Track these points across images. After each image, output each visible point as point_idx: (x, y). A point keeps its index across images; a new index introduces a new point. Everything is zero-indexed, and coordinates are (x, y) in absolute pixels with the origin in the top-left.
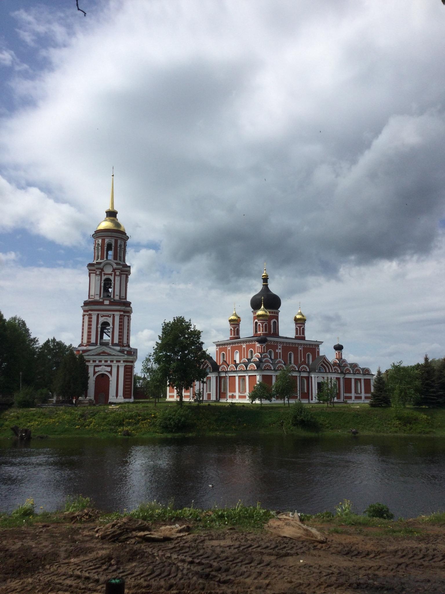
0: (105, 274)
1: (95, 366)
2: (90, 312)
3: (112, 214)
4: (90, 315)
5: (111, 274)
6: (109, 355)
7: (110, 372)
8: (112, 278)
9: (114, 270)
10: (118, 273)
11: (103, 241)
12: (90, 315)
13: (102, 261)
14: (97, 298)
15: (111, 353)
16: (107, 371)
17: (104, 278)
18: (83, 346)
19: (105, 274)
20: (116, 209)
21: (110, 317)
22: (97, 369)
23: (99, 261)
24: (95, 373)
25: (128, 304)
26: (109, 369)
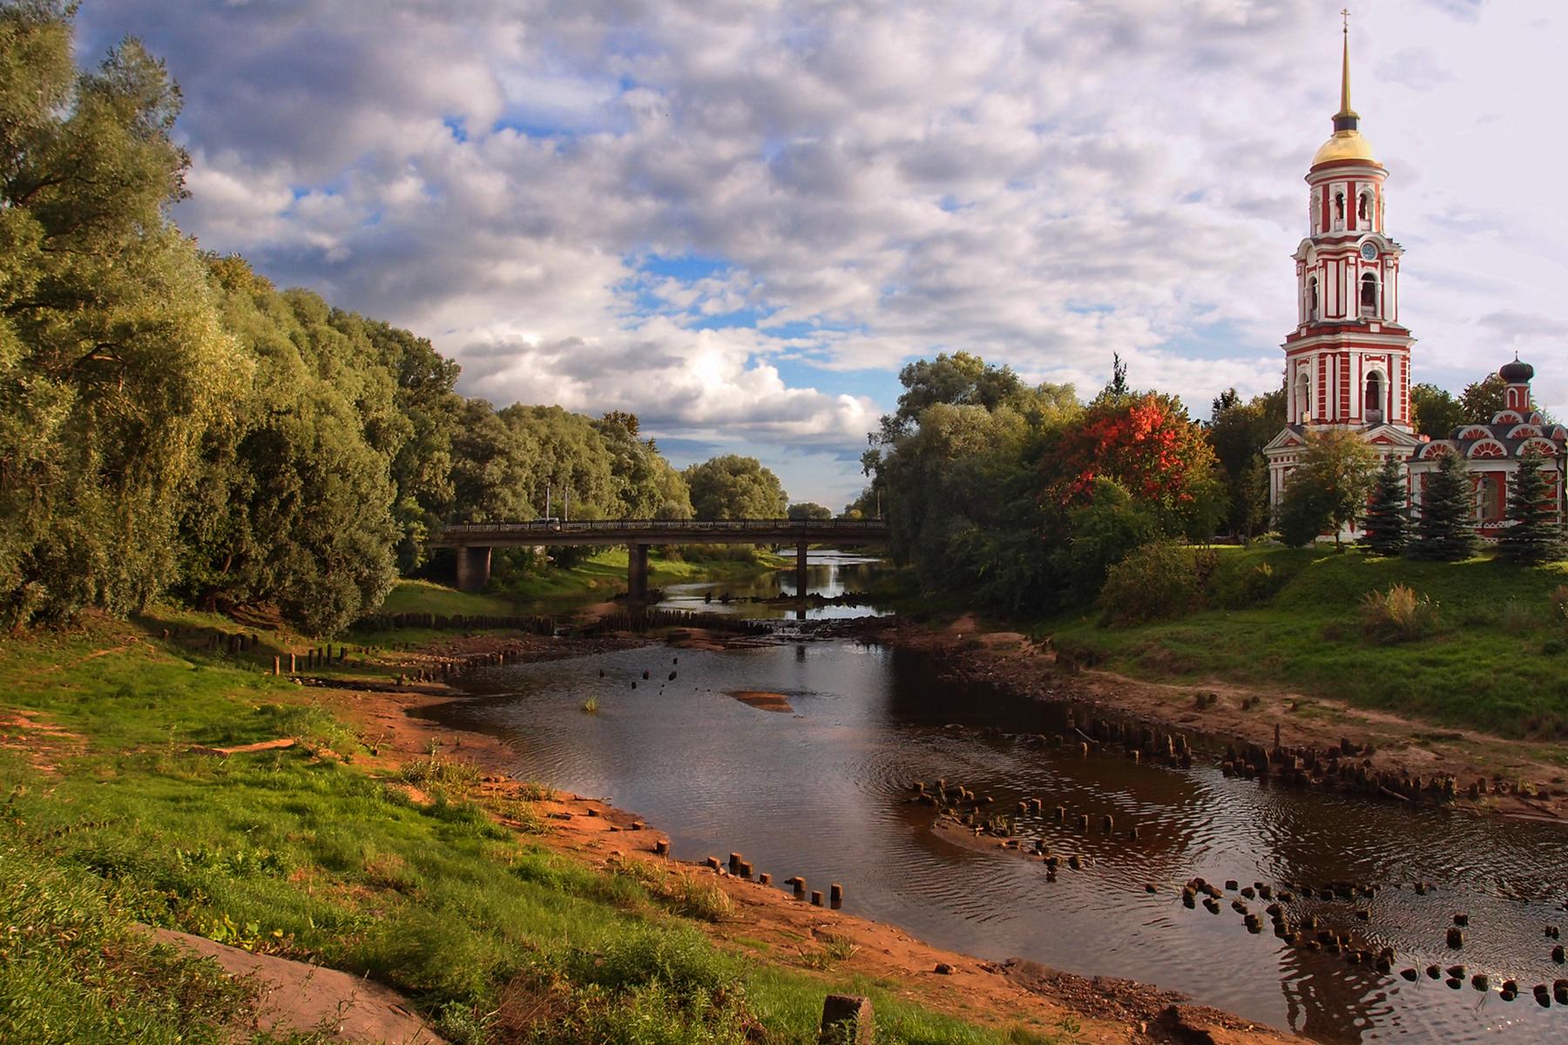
0: (1364, 264)
2: (1344, 350)
3: (1345, 123)
4: (1347, 354)
5: (1375, 265)
6: (1390, 442)
8: (1377, 273)
9: (1381, 256)
10: (1391, 263)
11: (1352, 187)
12: (1347, 354)
13: (1352, 233)
14: (1351, 317)
17: (1362, 271)
18: (1326, 422)
19: (1364, 264)
20: (1354, 107)
23: (1346, 232)
25: (1404, 332)
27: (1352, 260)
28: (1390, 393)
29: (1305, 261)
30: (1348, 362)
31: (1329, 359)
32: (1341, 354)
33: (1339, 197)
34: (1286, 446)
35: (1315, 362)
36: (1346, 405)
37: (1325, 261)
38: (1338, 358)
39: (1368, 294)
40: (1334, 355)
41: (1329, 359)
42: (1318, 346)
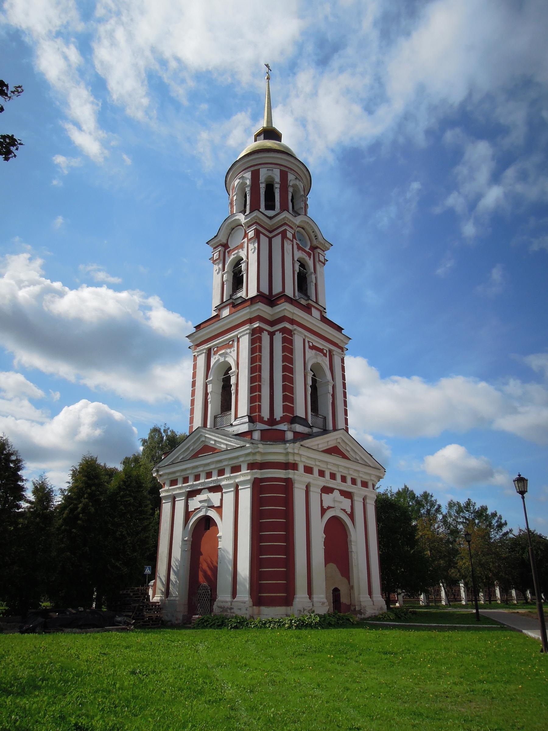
1: (327, 490)
4: (290, 332)
6: (345, 457)
7: (351, 516)
8: (310, 263)
11: (284, 176)
12: (290, 332)
15: (351, 455)
16: (344, 510)
21: (325, 355)
22: (328, 500)
24: (323, 511)
26: (346, 503)
27: (289, 235)
28: (333, 396)
29: (225, 246)
30: (291, 342)
31: (265, 338)
32: (284, 330)
33: (270, 188)
34: (195, 456)
35: (245, 342)
36: (288, 398)
37: (258, 233)
38: (278, 337)
39: (302, 281)
40: (272, 334)
41: (265, 338)
42: (251, 321)
